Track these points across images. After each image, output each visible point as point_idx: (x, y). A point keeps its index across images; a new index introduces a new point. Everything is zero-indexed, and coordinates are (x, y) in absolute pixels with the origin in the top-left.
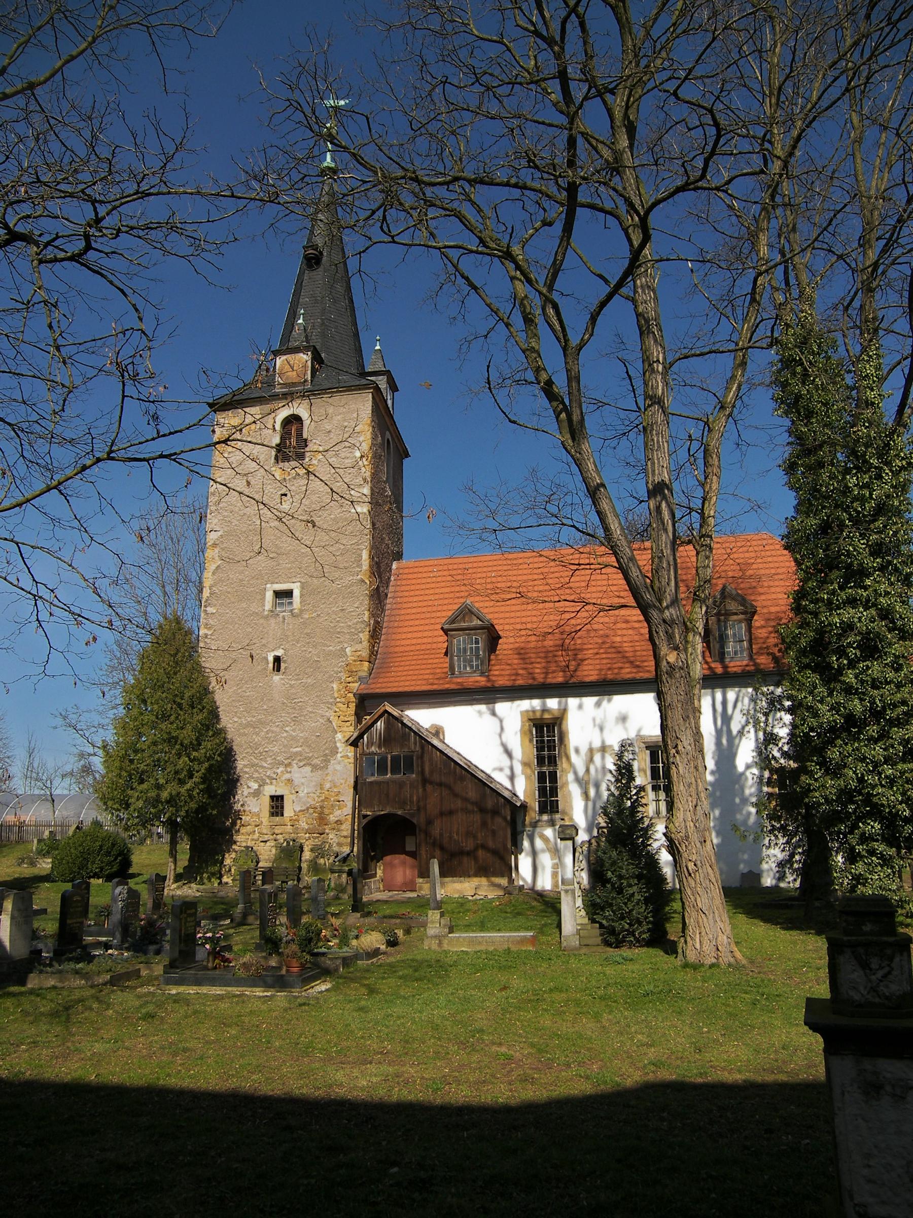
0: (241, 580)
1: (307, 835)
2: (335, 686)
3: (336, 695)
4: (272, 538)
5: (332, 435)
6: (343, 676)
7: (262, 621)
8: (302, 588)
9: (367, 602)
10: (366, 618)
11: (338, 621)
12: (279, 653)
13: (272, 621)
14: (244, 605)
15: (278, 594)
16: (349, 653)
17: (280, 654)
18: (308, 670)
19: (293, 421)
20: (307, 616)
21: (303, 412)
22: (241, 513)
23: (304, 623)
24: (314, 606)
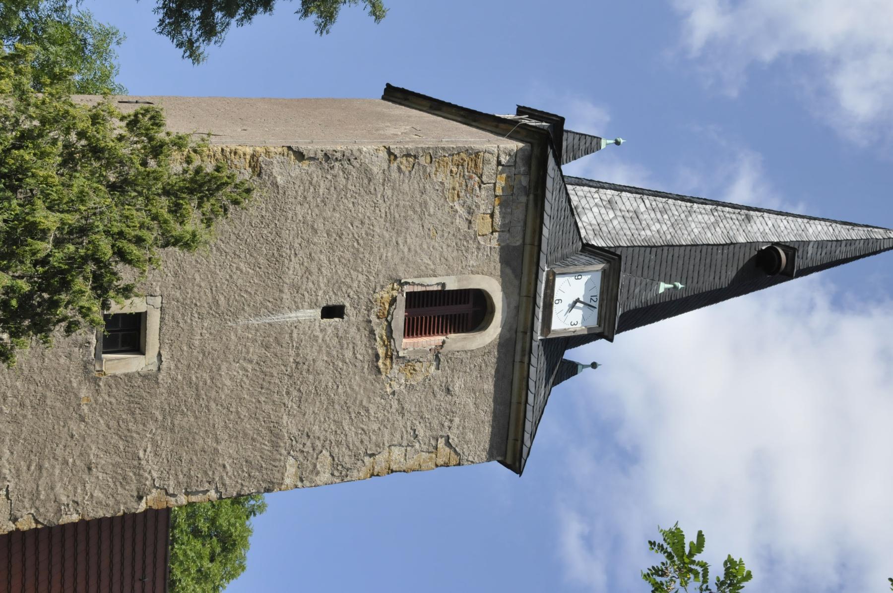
4: (259, 298)
5: (441, 395)
8: (145, 377)
9: (101, 514)
10: (65, 520)
11: (66, 462)
20: (84, 393)
22: (319, 225)
23: (68, 389)
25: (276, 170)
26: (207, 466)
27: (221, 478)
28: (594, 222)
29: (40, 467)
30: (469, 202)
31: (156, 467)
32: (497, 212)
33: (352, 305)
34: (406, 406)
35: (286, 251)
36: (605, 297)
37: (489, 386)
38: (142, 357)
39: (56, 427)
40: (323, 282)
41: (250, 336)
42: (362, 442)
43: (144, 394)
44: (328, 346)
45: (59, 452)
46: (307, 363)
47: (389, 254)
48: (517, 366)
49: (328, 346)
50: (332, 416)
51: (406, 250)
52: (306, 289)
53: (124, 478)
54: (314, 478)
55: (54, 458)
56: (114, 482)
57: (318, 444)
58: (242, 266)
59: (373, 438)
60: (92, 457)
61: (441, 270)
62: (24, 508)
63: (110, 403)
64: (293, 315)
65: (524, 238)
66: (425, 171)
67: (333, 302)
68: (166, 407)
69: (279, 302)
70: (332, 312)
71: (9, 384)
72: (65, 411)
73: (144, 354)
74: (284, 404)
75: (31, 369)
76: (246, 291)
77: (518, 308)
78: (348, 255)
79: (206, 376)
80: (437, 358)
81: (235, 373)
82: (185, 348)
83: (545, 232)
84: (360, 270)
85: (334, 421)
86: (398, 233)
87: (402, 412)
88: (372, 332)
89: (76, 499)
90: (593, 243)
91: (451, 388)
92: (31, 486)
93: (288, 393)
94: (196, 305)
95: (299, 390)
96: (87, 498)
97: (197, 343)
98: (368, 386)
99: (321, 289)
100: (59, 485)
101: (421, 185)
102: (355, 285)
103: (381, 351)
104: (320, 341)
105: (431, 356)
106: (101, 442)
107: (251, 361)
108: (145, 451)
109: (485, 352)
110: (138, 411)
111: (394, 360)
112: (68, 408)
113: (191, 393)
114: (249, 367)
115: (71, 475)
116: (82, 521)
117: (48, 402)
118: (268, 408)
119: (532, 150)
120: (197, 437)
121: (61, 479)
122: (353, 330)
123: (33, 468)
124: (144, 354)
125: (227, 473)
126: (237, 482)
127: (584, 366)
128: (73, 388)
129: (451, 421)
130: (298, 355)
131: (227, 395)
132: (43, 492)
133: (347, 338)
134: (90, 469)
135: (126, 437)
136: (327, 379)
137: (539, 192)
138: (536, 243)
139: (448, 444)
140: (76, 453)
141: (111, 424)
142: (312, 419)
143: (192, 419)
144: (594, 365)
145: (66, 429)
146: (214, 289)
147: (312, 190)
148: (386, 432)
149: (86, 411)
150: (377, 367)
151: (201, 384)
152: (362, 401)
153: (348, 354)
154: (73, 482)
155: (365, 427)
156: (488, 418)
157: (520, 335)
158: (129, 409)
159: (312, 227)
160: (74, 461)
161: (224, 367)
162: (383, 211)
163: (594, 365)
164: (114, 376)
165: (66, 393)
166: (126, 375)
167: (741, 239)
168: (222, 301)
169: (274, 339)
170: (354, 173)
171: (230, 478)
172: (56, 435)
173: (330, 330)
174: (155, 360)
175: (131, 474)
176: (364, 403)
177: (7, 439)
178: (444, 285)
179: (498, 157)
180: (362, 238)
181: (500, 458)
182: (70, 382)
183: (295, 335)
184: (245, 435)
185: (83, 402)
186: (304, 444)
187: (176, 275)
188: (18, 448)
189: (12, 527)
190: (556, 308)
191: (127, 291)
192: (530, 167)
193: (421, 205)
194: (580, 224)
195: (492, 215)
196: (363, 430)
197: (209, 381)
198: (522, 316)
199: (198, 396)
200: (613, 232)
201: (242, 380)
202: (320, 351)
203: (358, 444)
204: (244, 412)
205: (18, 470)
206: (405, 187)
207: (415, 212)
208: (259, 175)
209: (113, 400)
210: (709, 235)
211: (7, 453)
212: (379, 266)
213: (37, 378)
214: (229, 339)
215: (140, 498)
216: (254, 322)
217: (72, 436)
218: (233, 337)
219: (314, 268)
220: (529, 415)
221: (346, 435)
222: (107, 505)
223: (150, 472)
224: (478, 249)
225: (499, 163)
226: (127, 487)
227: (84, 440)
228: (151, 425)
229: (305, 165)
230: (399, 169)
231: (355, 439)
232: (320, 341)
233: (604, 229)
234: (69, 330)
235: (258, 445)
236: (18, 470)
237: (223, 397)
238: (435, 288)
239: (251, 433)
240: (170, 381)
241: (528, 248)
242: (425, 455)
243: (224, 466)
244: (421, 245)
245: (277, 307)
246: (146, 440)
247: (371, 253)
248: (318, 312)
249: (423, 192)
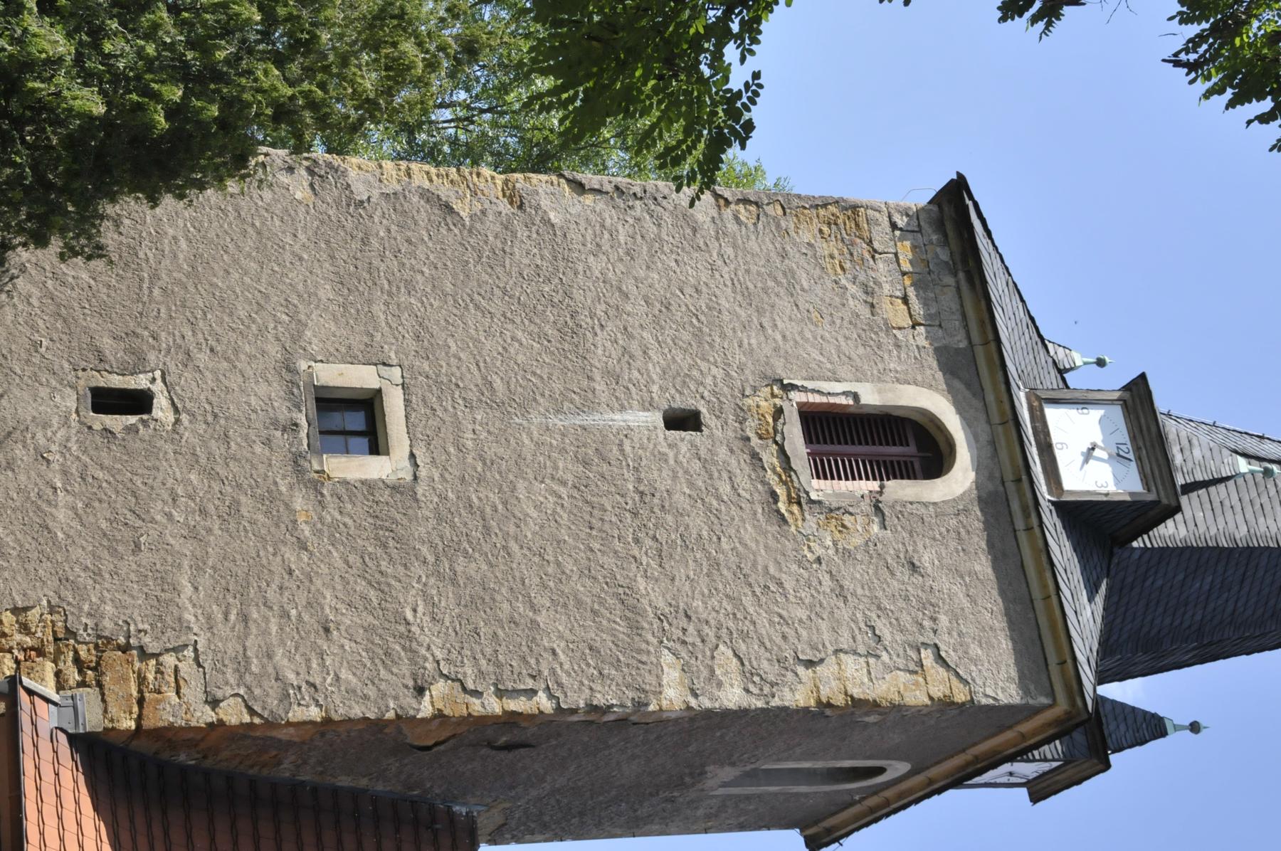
0: (410, 286)
4: (557, 386)
5: (903, 573)
7: (274, 350)
8: (395, 488)
9: (357, 711)
10: (297, 714)
11: (285, 615)
12: (161, 409)
13: (276, 390)
14: (326, 291)
17: (156, 413)
18: (103, 511)
20: (298, 503)
21: (961, 477)
22: (628, 285)
24: (334, 526)
25: (545, 203)
26: (524, 648)
27: (553, 672)
29: (245, 618)
30: (862, 277)
31: (439, 641)
32: (912, 293)
33: (711, 410)
34: (846, 583)
35: (584, 319)
36: (1141, 444)
37: (983, 566)
38: (384, 458)
39: (262, 553)
40: (655, 372)
41: (554, 443)
42: (784, 637)
43: (398, 517)
44: (686, 472)
45: (271, 594)
46: (658, 495)
47: (753, 341)
48: (1023, 537)
49: (686, 472)
50: (720, 587)
51: (779, 337)
52: (630, 379)
54: (717, 693)
55: (265, 604)
56: (372, 659)
57: (710, 632)
58: (519, 334)
59: (804, 633)
60: (327, 611)
61: (843, 371)
62: (227, 683)
63: (345, 524)
64: (617, 416)
66: (778, 226)
67: (680, 403)
68: (437, 541)
69: (590, 395)
70: (682, 421)
71: (178, 475)
72: (272, 529)
73: (387, 453)
74: (634, 557)
75: (210, 456)
76: (534, 373)
77: (993, 443)
78: (686, 336)
79: (495, 498)
80: (878, 509)
81: (542, 499)
82: (452, 450)
84: (711, 359)
85: (727, 596)
86: (760, 312)
87: (841, 593)
88: (755, 456)
89: (311, 680)
91: (917, 563)
92: (232, 648)
93: (637, 541)
94: (457, 386)
95: (654, 538)
96: (329, 680)
97: (470, 444)
98: (771, 542)
99: (653, 382)
100: (279, 652)
101: (778, 246)
102: (709, 380)
104: (672, 462)
105: (866, 506)
106: (339, 587)
107: (563, 483)
108: (415, 611)
109: (957, 508)
110: (391, 543)
111: (805, 507)
112: (277, 526)
113: (474, 523)
114: (563, 491)
115: (297, 637)
116: (327, 721)
117: (244, 511)
118: (609, 561)
120: (498, 598)
121: (282, 643)
122: (723, 452)
123: (233, 617)
124: (387, 453)
125: (561, 664)
126: (582, 683)
127: (1177, 728)
128: (281, 494)
130: (639, 480)
131: (534, 533)
132: (255, 661)
133: (715, 463)
134: (327, 630)
135: (378, 583)
136: (697, 523)
137: (971, 263)
138: (991, 337)
139: (940, 659)
140: (302, 599)
141: (351, 559)
142: (687, 587)
143: (484, 567)
144: (1195, 727)
145: (279, 558)
146: (482, 365)
147: (606, 236)
148: (824, 626)
149: (307, 533)
150: (778, 511)
151: (488, 509)
152: (766, 568)
153: (725, 489)
154: (301, 649)
155: (784, 613)
156: (1000, 623)
157: (1011, 487)
158: (377, 538)
159: (620, 289)
160: (299, 615)
161: (521, 485)
162: (726, 276)
163: (1195, 727)
164: (345, 483)
165: (270, 498)
166: (363, 482)
168: (498, 383)
169: (596, 452)
170: (666, 216)
171: (569, 675)
172: (263, 566)
173: (684, 448)
174: (406, 463)
175: (398, 648)
176: (772, 570)
177: (186, 563)
178: (856, 396)
179: (890, 217)
180: (703, 313)
182: (276, 483)
183: (628, 449)
184: (579, 603)
185: (301, 519)
186: (684, 630)
187: (418, 337)
188: (205, 581)
189: (209, 716)
190: (1060, 455)
192: (946, 236)
193: (785, 274)
195: (905, 300)
196: (781, 617)
197: (500, 507)
198: (1004, 454)
199: (487, 528)
201: (554, 511)
202: (675, 477)
203: (779, 640)
204: (569, 566)
205: (209, 618)
206: (753, 245)
207: (778, 283)
208: (521, 207)
209: (350, 522)
211: (188, 590)
212: (740, 357)
213: (223, 473)
214: (520, 443)
215: (420, 691)
216: (556, 421)
217: (290, 572)
218: (527, 442)
219: (634, 347)
221: (754, 623)
222: (366, 697)
223: (429, 648)
225: (894, 226)
226: (395, 670)
227: (311, 581)
228: (417, 569)
229: (589, 199)
230: (737, 218)
231: (772, 631)
232: (672, 462)
235: (605, 622)
236: (209, 618)
237: (530, 536)
238: (843, 400)
239: (589, 600)
240: (436, 499)
241: (980, 351)
242: (903, 677)
243: (554, 652)
244: (801, 333)
245: (589, 403)
246: (413, 592)
247: (723, 336)
248: (657, 418)
249: (784, 255)
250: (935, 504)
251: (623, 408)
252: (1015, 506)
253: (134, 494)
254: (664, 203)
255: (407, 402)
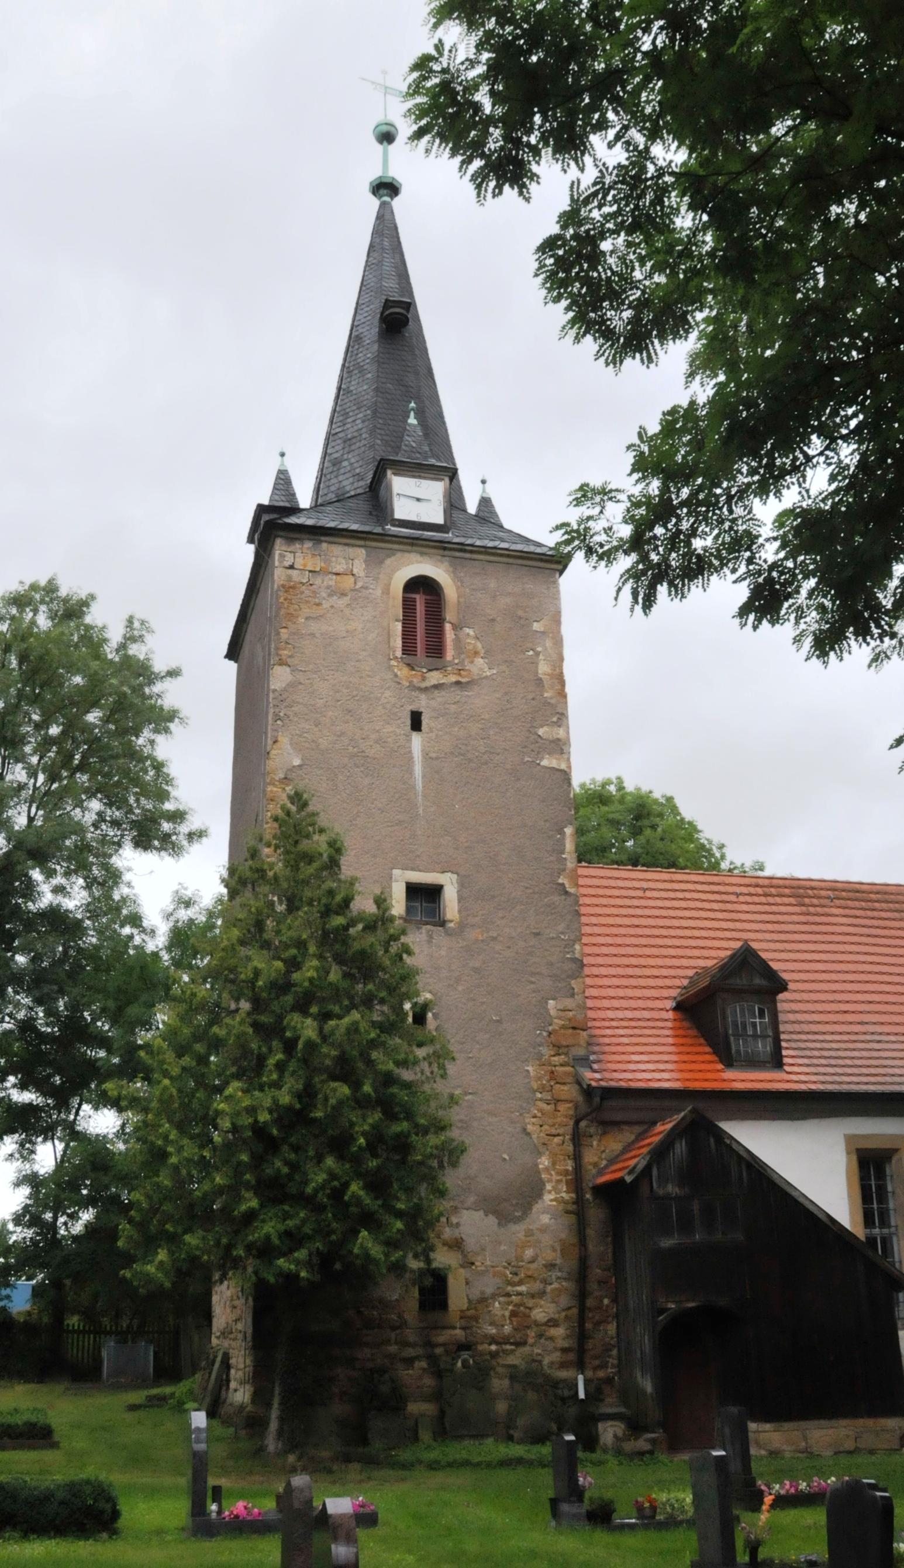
1: (493, 1347)
2: (530, 1068)
3: (535, 1086)
6: (546, 1051)
8: (462, 885)
15: (414, 891)
16: (553, 1012)
19: (421, 585)
28: (351, 480)
29: (533, 974)
30: (324, 595)
51: (364, 653)
53: (549, 906)
65: (360, 546)
66: (294, 634)
77: (422, 554)
83: (354, 527)
88: (437, 687)
90: (369, 482)
95: (484, 753)
103: (453, 678)
119: (281, 537)
122: (433, 703)
123: (533, 979)
127: (484, 491)
129: (520, 618)
134: (538, 934)
141: (501, 915)
153: (453, 708)
157: (447, 553)
159: (339, 736)
164: (460, 911)
166: (459, 902)
167: (376, 347)
181: (557, 575)
183: (434, 755)
187: (374, 856)
191: (381, 902)
192: (297, 539)
194: (353, 493)
200: (360, 463)
203: (534, 703)
205: (534, 992)
210: (369, 375)
218: (432, 809)
220: (519, 547)
224: (367, 588)
230: (290, 657)
233: (358, 471)
234: (409, 953)
241: (368, 543)
250: (459, 597)
251: (410, 752)
252: (458, 554)
253: (471, 1020)
254: (284, 696)
255: (413, 869)
